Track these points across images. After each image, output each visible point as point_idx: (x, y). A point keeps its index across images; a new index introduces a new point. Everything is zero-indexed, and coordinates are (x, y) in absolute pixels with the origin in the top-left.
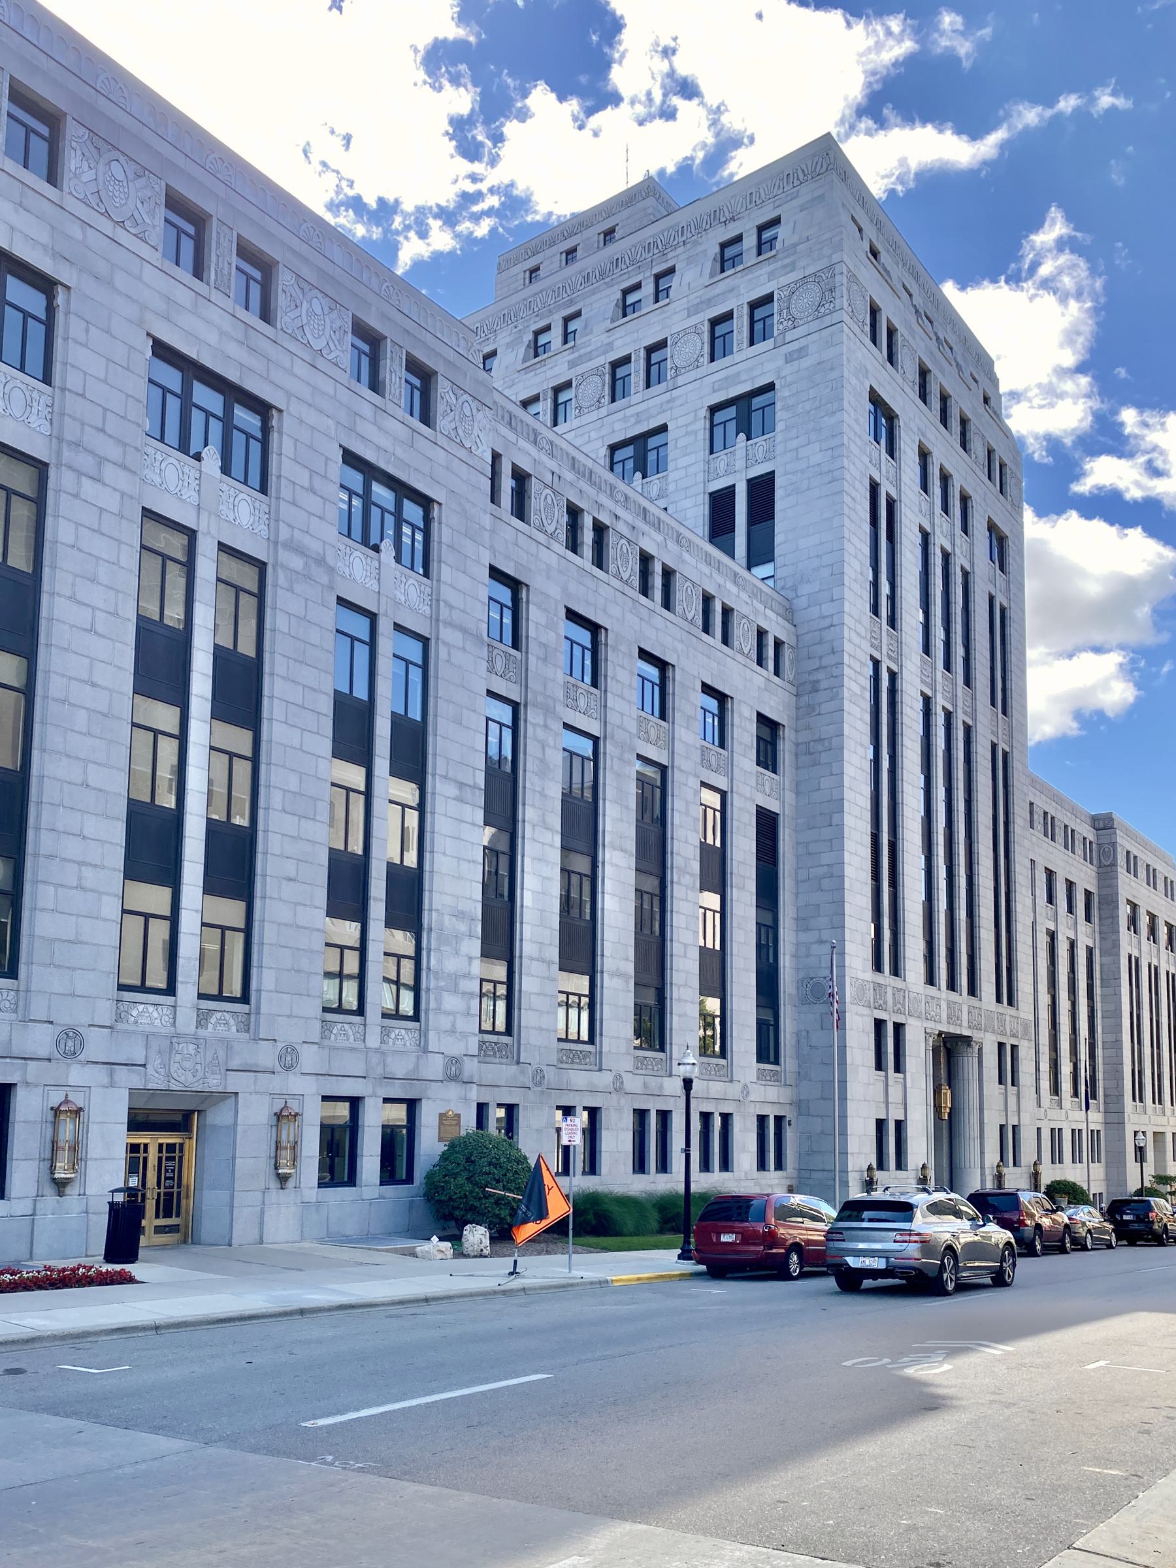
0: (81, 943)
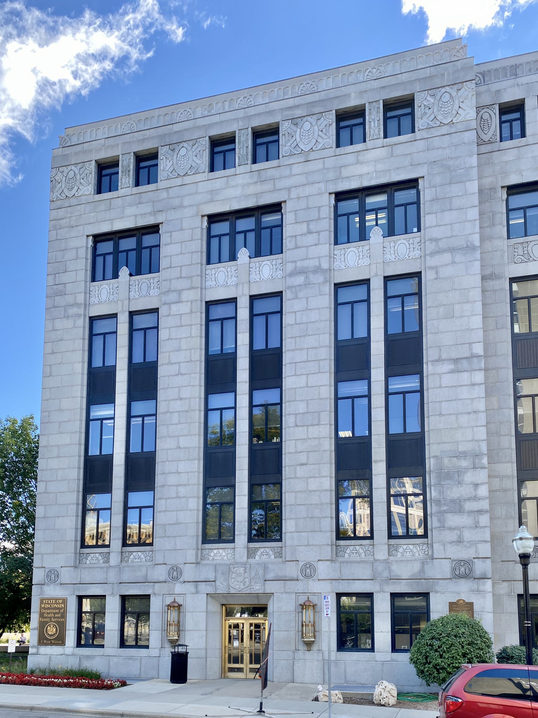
0: (179, 523)
